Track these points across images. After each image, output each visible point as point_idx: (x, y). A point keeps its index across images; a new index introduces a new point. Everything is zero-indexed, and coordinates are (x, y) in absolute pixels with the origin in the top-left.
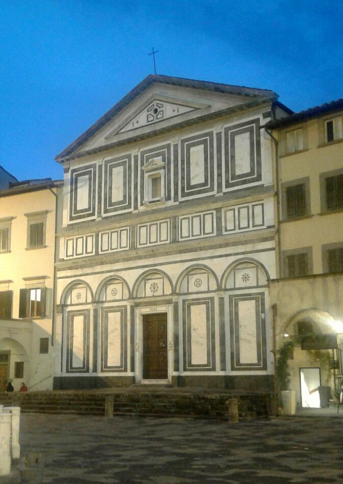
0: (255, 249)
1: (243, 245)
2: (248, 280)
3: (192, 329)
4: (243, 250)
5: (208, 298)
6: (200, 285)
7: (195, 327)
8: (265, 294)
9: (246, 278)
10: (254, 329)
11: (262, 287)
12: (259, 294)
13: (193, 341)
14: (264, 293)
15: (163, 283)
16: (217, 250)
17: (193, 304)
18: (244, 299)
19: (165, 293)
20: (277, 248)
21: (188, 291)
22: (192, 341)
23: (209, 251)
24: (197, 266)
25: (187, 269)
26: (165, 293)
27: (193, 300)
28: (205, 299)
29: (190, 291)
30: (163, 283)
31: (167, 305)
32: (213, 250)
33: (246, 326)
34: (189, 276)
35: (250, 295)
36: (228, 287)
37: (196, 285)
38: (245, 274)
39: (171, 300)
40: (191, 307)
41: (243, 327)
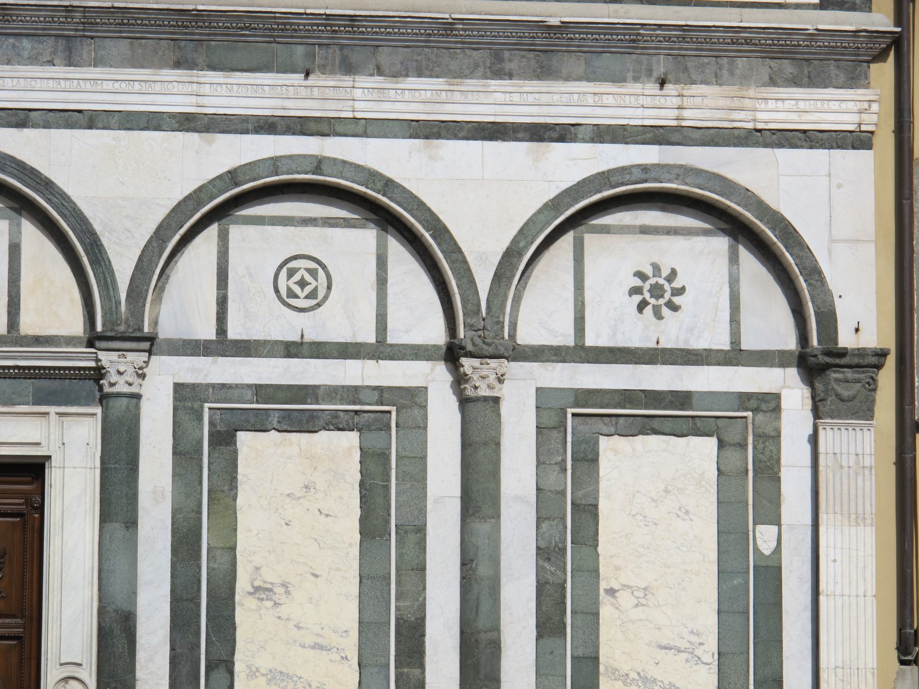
0: (744, 120)
1: (662, 83)
2: (674, 308)
3: (242, 584)
4: (665, 118)
5: (383, 393)
6: (317, 301)
7: (269, 576)
8: (784, 405)
9: (657, 290)
10: (708, 621)
11: (762, 359)
12: (745, 400)
13: (253, 673)
14: (777, 397)
15: (15, 250)
16: (472, 84)
17: (258, 423)
18: (648, 426)
19: (29, 324)
20: (886, 141)
21: (221, 329)
22: (238, 667)
23: (413, 82)
24: (318, 170)
25: (233, 176)
26: (29, 324)
27: (262, 392)
28: (353, 393)
29: (234, 333)
30: (15, 250)
31: (53, 409)
32: (439, 83)
33: (645, 589)
34: (236, 232)
35: (682, 399)
36: (527, 335)
37: (286, 299)
38: (673, 274)
39: (98, 373)
40: (241, 436)
41: (624, 598)
